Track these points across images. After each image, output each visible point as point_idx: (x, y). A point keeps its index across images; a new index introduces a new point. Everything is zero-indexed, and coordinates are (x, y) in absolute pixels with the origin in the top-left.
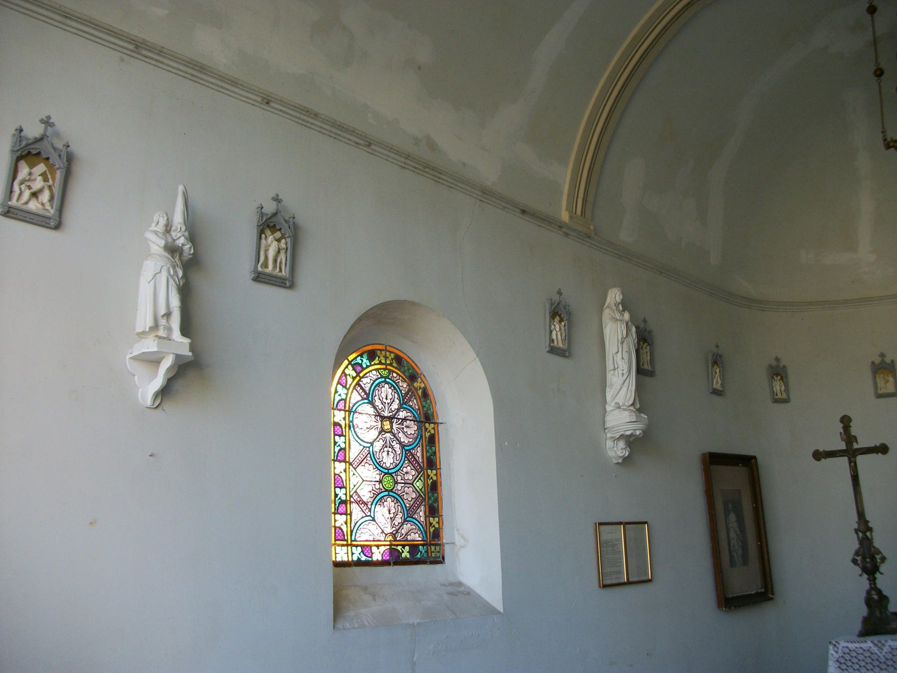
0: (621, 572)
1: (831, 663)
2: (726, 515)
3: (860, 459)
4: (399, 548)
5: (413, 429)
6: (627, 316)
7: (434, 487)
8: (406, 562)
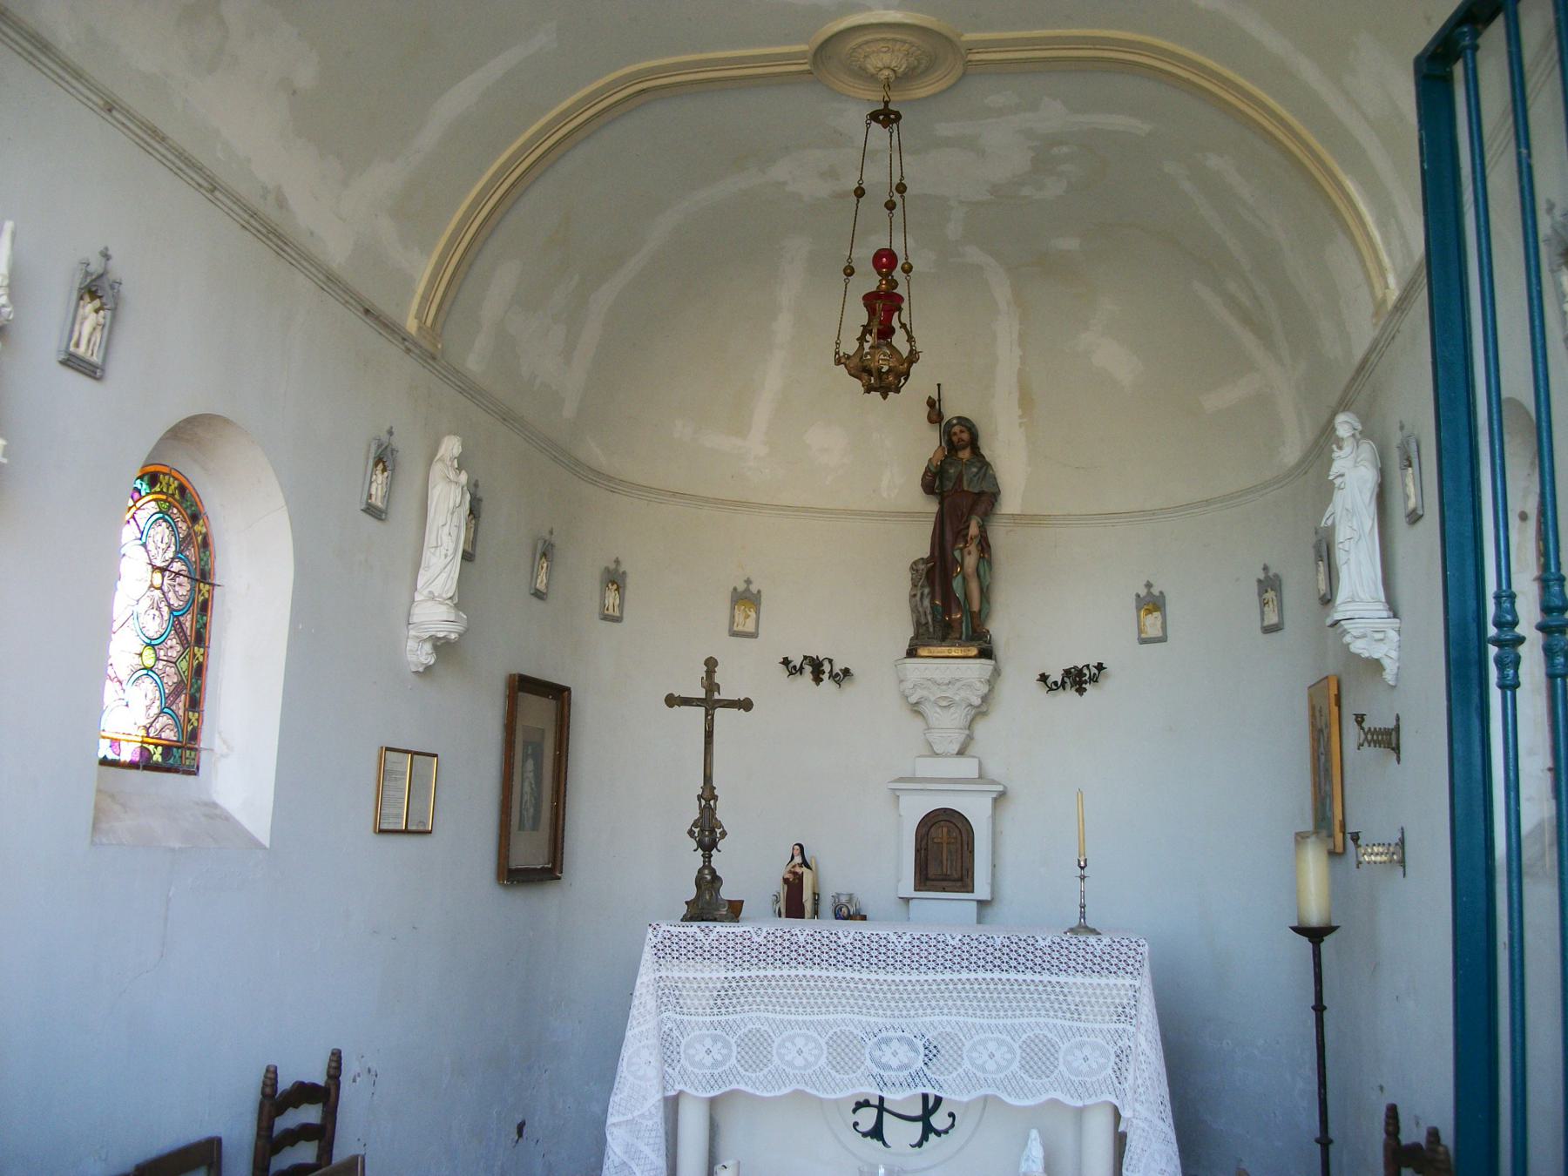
0: (399, 816)
1: (647, 949)
2: (524, 761)
3: (720, 713)
4: (151, 748)
5: (184, 588)
6: (463, 478)
7: (199, 671)
8: (156, 768)
